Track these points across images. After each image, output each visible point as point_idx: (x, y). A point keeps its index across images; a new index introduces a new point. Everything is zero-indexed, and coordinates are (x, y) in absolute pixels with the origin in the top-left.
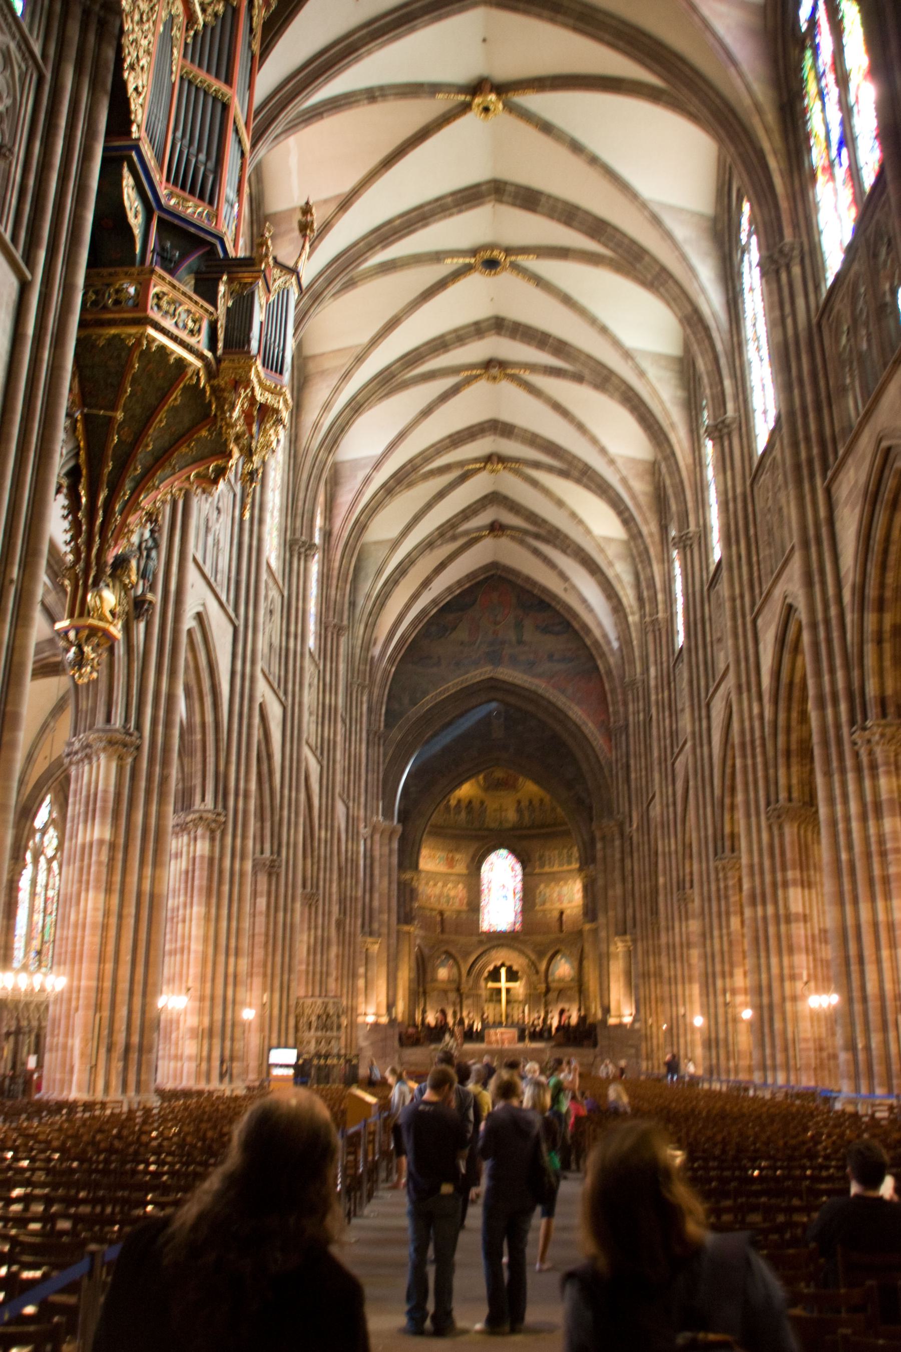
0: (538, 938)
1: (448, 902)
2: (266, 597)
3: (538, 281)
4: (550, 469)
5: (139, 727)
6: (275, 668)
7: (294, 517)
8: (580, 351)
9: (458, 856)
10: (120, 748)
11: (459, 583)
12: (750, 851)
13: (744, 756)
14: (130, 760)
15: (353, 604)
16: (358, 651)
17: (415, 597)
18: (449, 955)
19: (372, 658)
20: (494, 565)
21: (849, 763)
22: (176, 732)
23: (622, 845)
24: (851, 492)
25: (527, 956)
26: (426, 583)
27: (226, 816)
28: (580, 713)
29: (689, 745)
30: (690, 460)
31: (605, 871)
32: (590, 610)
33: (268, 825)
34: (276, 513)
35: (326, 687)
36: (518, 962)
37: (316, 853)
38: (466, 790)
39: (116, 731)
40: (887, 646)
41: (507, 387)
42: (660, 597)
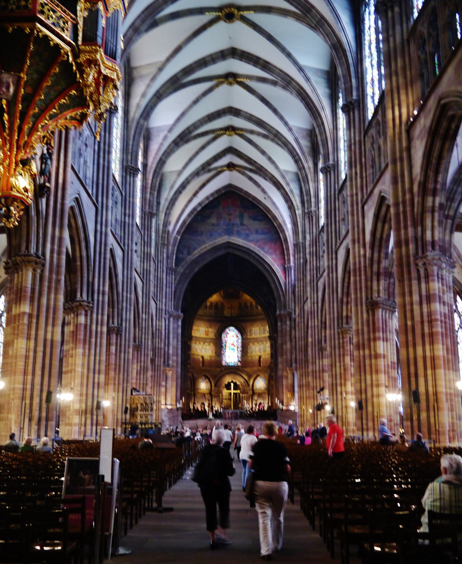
1: (205, 352)
2: (113, 195)
4: (259, 134)
5: (44, 254)
6: (118, 232)
9: (210, 330)
10: (34, 264)
11: (212, 195)
13: (355, 276)
14: (39, 271)
15: (158, 203)
16: (161, 227)
17: (190, 201)
18: (206, 377)
19: (168, 231)
20: (230, 186)
22: (64, 257)
23: (291, 325)
24: (421, 132)
26: (195, 194)
27: (93, 304)
29: (326, 271)
30: (331, 127)
31: (282, 337)
32: (277, 208)
33: (116, 310)
34: (118, 151)
35: (146, 243)
37: (141, 326)
38: (215, 298)
39: (31, 255)
40: (436, 215)
42: (313, 200)
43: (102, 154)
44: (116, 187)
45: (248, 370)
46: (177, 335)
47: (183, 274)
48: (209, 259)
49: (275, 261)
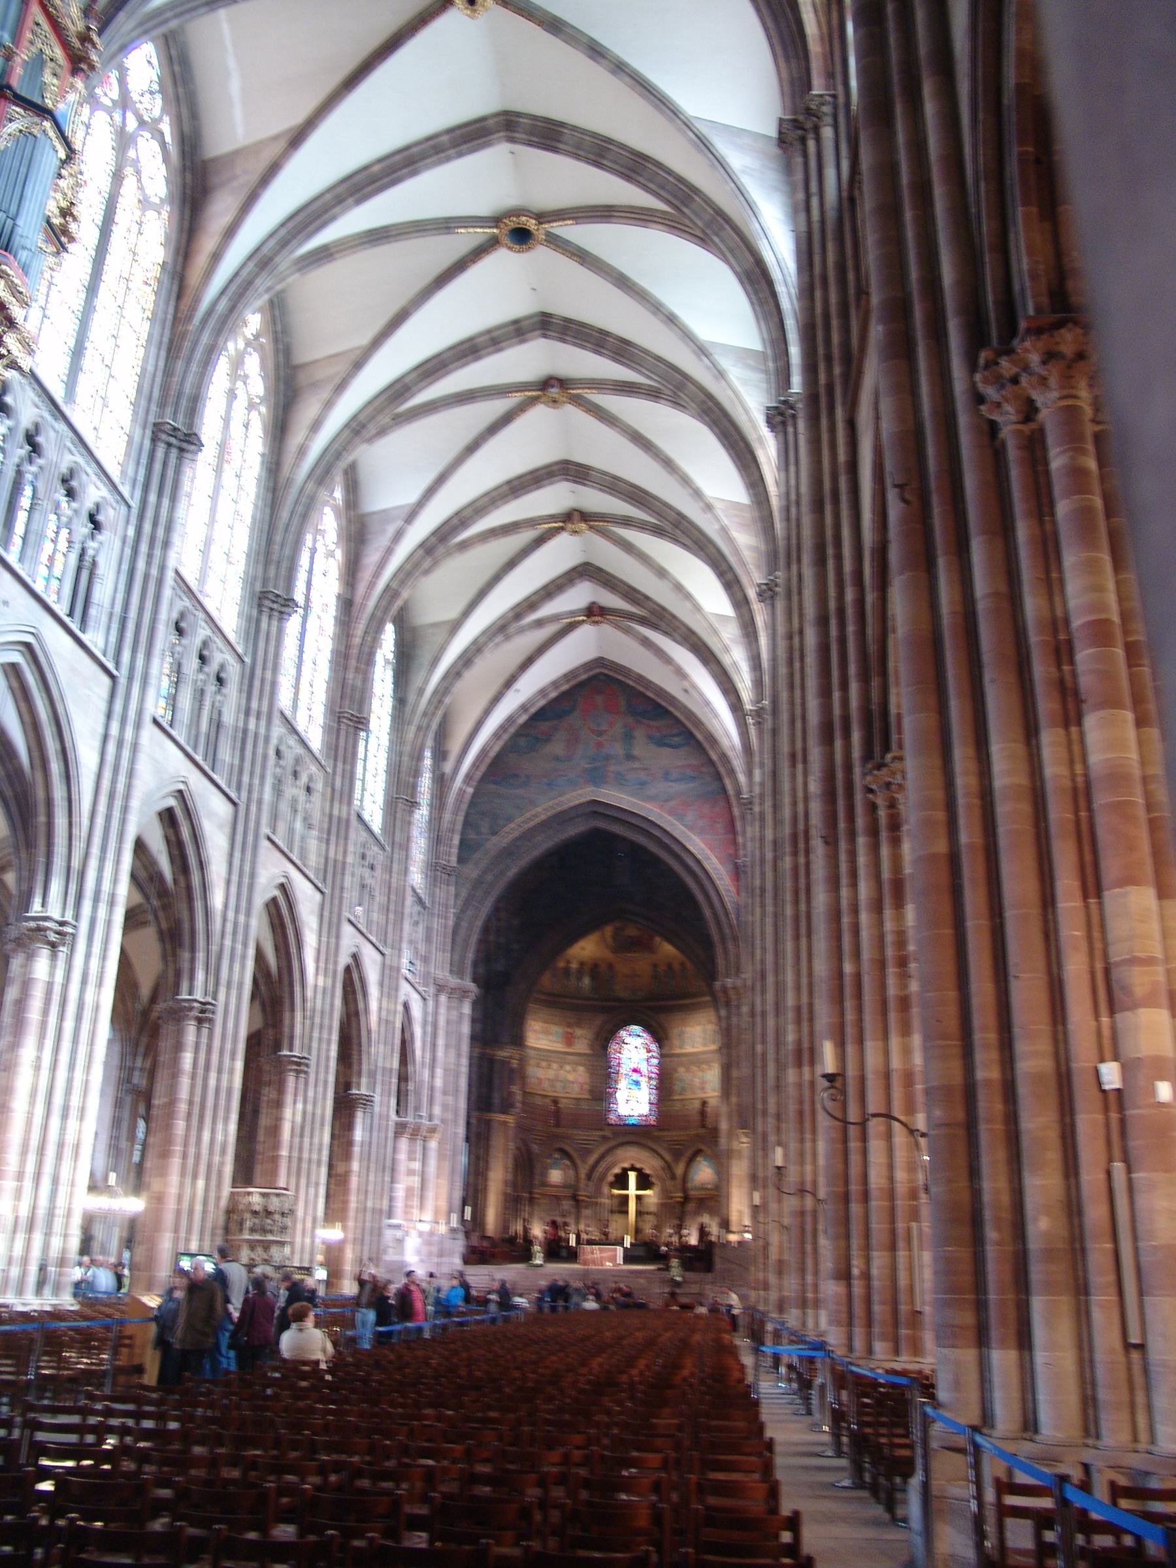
0: (674, 1134)
3: (582, 257)
4: (643, 526)
7: (267, 563)
8: (646, 352)
9: (579, 1032)
11: (555, 684)
12: (798, 988)
18: (565, 1154)
19: (443, 775)
20: (600, 662)
21: (860, 822)
25: (662, 1158)
28: (702, 845)
32: (716, 716)
33: (201, 956)
36: (650, 1165)
37: (309, 1005)
38: (587, 949)
41: (571, 411)
43: (144, 548)
44: (219, 642)
45: (674, 1134)
46: (459, 1039)
47: (478, 883)
48: (544, 844)
49: (711, 849)
